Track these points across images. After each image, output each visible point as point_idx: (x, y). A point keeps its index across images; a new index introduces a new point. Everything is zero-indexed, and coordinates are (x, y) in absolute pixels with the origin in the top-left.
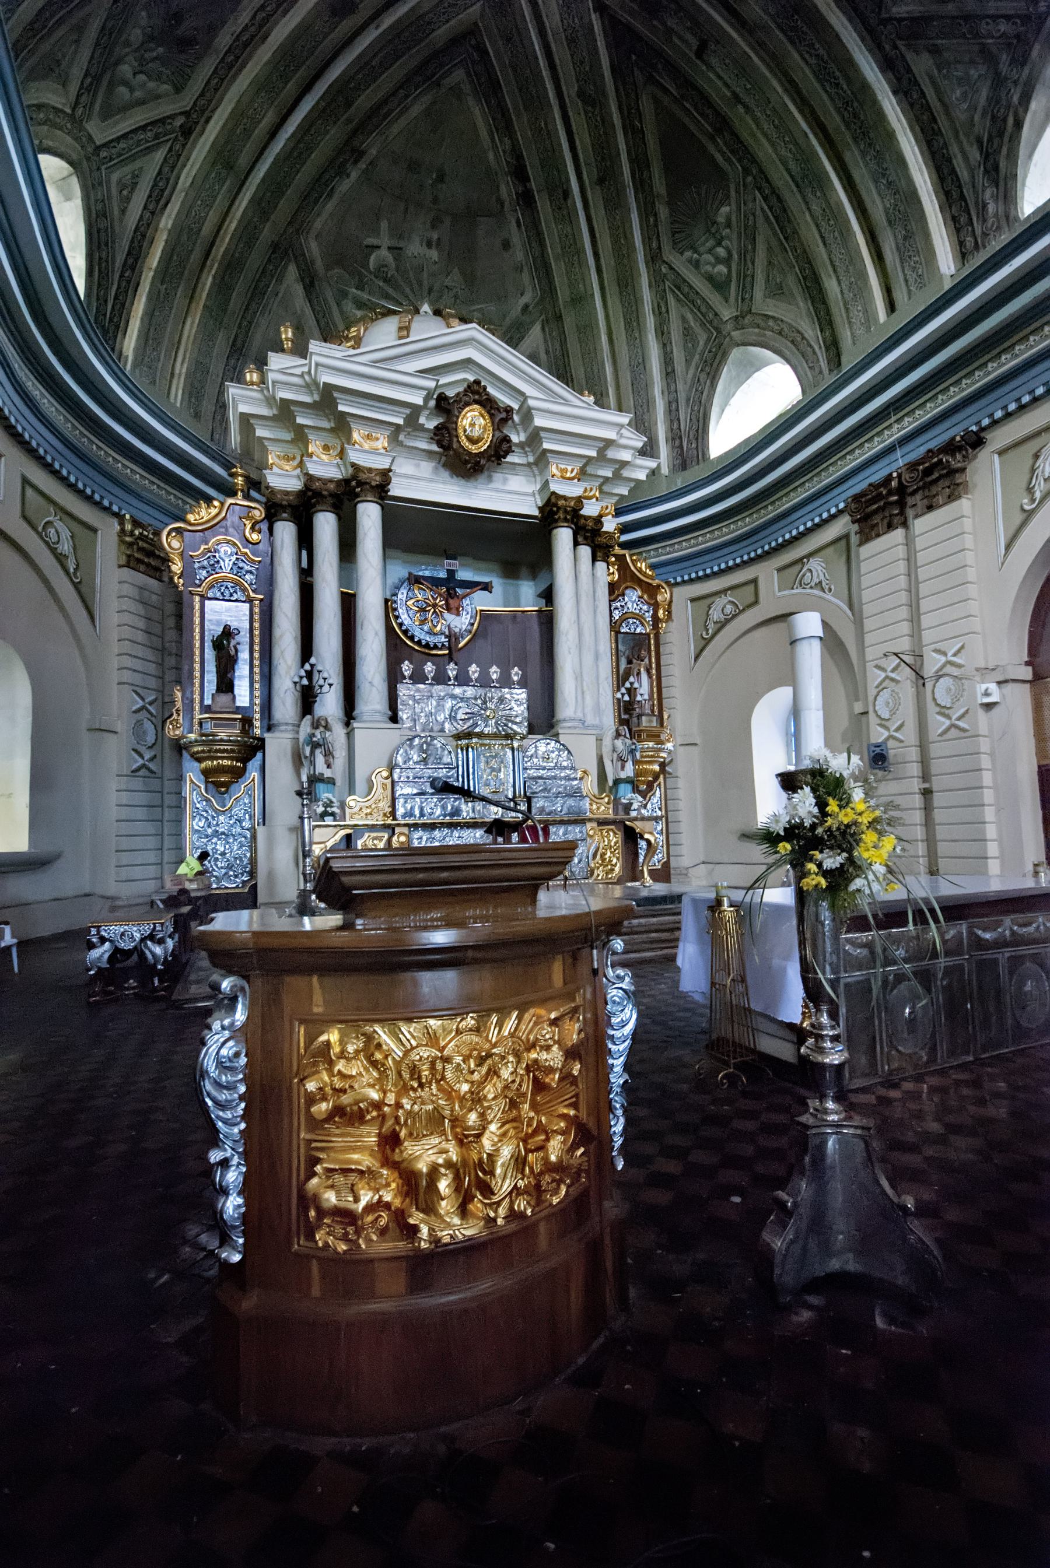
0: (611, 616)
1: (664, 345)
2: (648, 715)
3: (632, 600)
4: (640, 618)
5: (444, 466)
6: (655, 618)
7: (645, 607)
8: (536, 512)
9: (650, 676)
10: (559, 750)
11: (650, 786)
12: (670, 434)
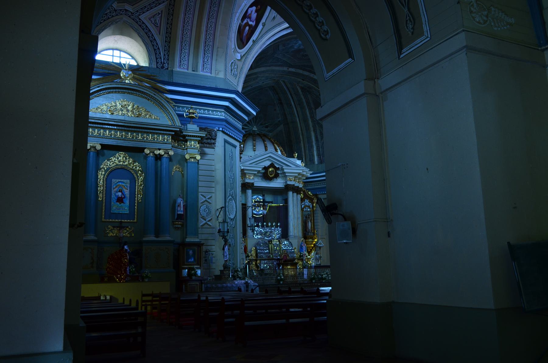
0: (301, 207)
1: (315, 134)
2: (310, 232)
3: (307, 202)
4: (309, 207)
5: (264, 178)
6: (313, 206)
7: (310, 204)
8: (284, 187)
9: (311, 222)
10: (289, 243)
11: (311, 250)
12: (317, 154)
